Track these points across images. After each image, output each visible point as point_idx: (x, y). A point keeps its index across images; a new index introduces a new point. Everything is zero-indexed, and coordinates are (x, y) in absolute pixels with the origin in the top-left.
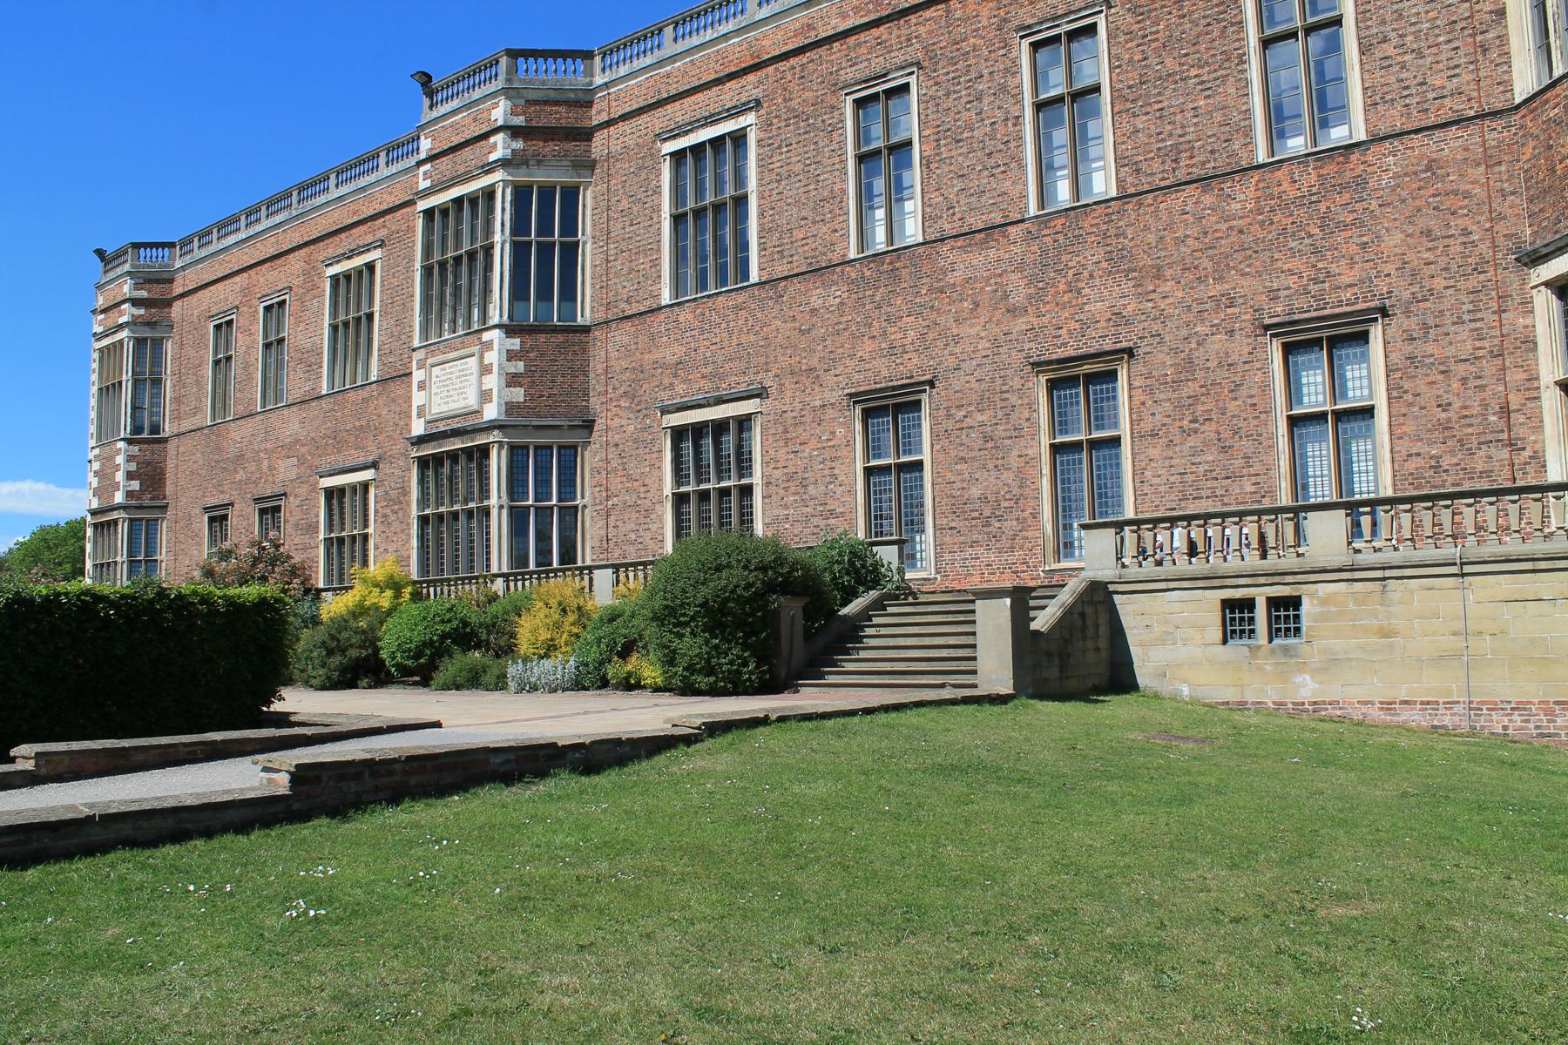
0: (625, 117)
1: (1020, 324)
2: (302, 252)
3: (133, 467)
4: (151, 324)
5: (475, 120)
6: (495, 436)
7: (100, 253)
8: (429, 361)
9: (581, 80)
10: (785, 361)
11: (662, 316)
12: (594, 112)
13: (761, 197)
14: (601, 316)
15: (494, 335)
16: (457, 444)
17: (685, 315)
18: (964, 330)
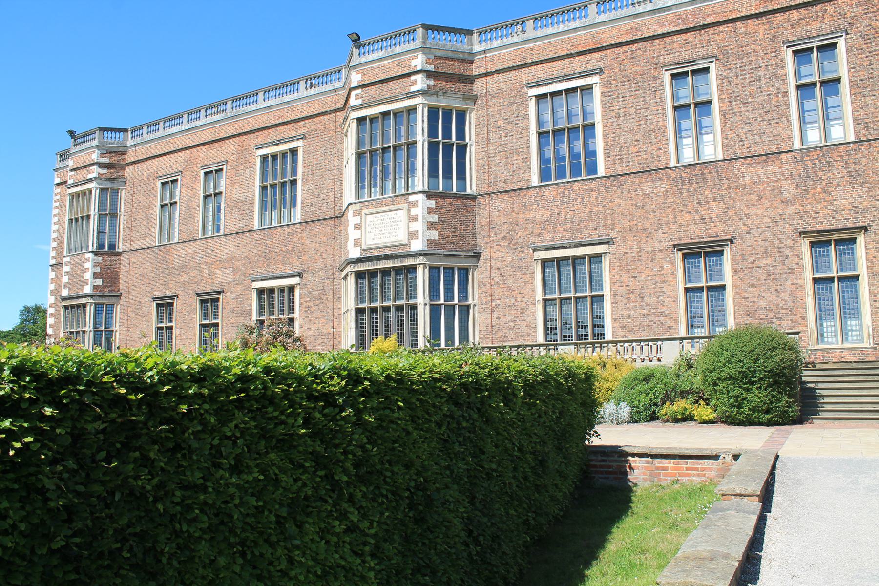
0: (498, 72)
1: (790, 210)
2: (237, 139)
3: (98, 270)
4: (111, 180)
5: (398, 65)
6: (421, 260)
7: (71, 133)
8: (364, 212)
9: (466, 47)
10: (625, 223)
11: (532, 192)
12: (474, 66)
13: (605, 125)
14: (484, 189)
15: (421, 198)
16: (389, 264)
17: (550, 193)
18: (752, 212)
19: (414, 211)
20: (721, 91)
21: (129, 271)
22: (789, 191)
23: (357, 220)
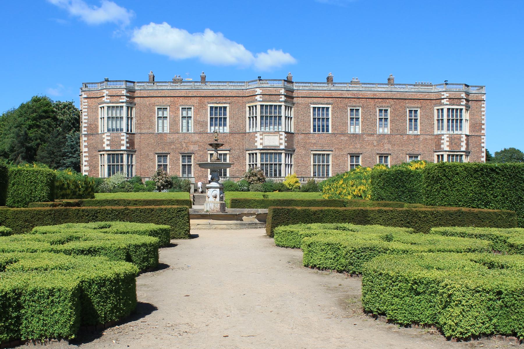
0: (302, 97)
1: (375, 148)
4: (131, 103)
6: (283, 151)
16: (273, 151)
17: (316, 135)
19: (281, 137)
20: (362, 116)
21: (140, 141)
22: (375, 144)
23: (261, 137)
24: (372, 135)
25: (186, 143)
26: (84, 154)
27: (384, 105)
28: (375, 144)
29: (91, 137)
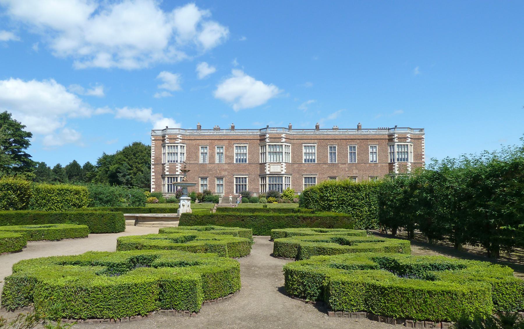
22: (347, 169)
24: (345, 164)
25: (220, 170)
26: (152, 177)
27: (353, 144)
28: (347, 169)
29: (157, 166)
